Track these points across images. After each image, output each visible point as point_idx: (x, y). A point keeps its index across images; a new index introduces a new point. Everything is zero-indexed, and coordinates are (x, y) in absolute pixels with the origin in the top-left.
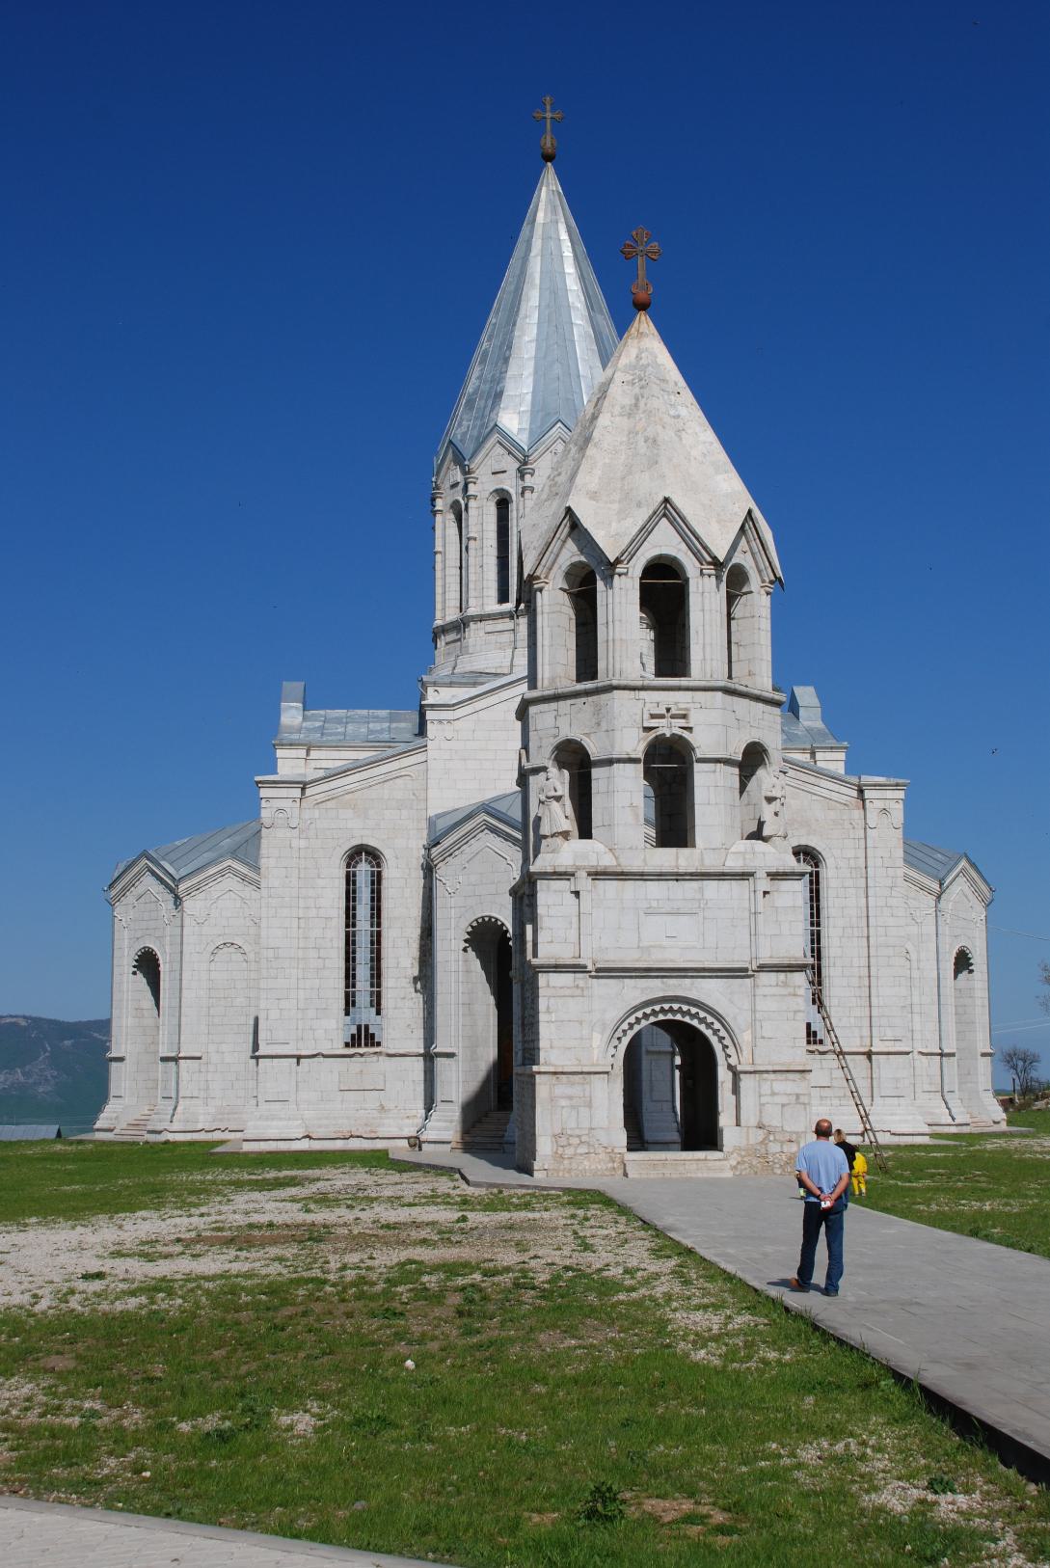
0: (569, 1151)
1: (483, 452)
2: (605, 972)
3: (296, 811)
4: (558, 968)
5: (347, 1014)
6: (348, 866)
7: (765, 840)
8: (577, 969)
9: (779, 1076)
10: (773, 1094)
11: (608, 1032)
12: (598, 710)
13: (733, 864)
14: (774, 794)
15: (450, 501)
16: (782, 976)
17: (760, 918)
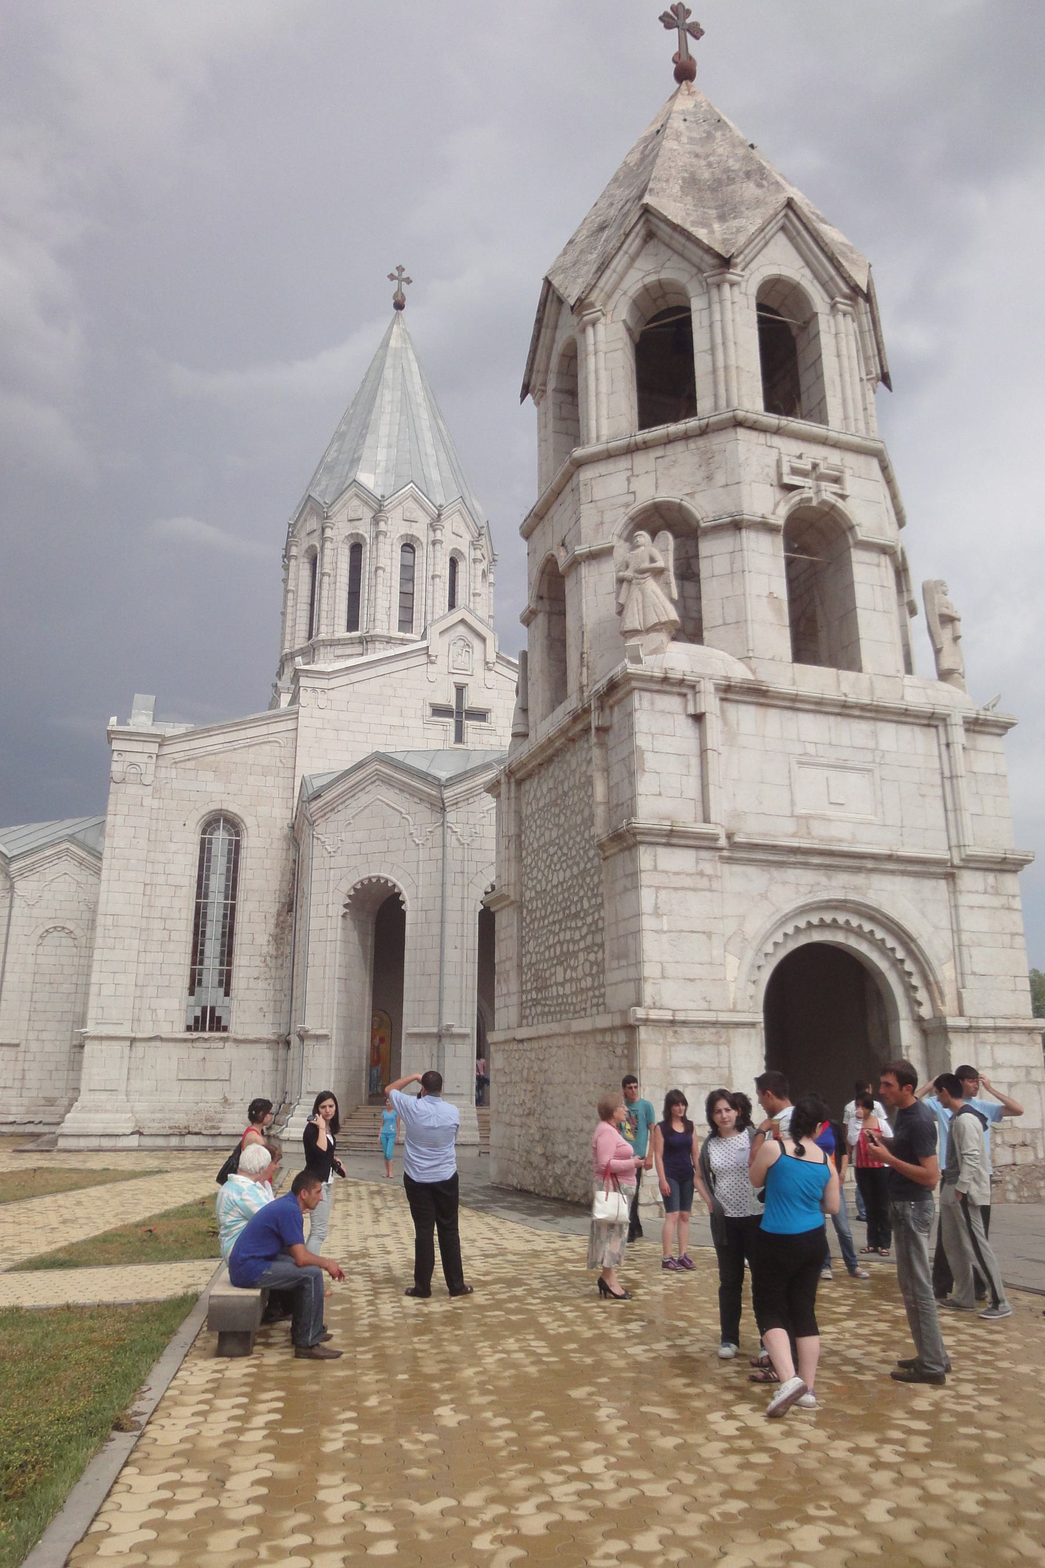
1: (341, 502)
2: (741, 851)
3: (151, 768)
4: (672, 837)
5: (192, 993)
6: (204, 832)
8: (703, 843)
9: (1004, 1038)
10: (996, 1066)
11: (750, 954)
12: (707, 459)
15: (305, 546)
16: (991, 878)
17: (962, 784)
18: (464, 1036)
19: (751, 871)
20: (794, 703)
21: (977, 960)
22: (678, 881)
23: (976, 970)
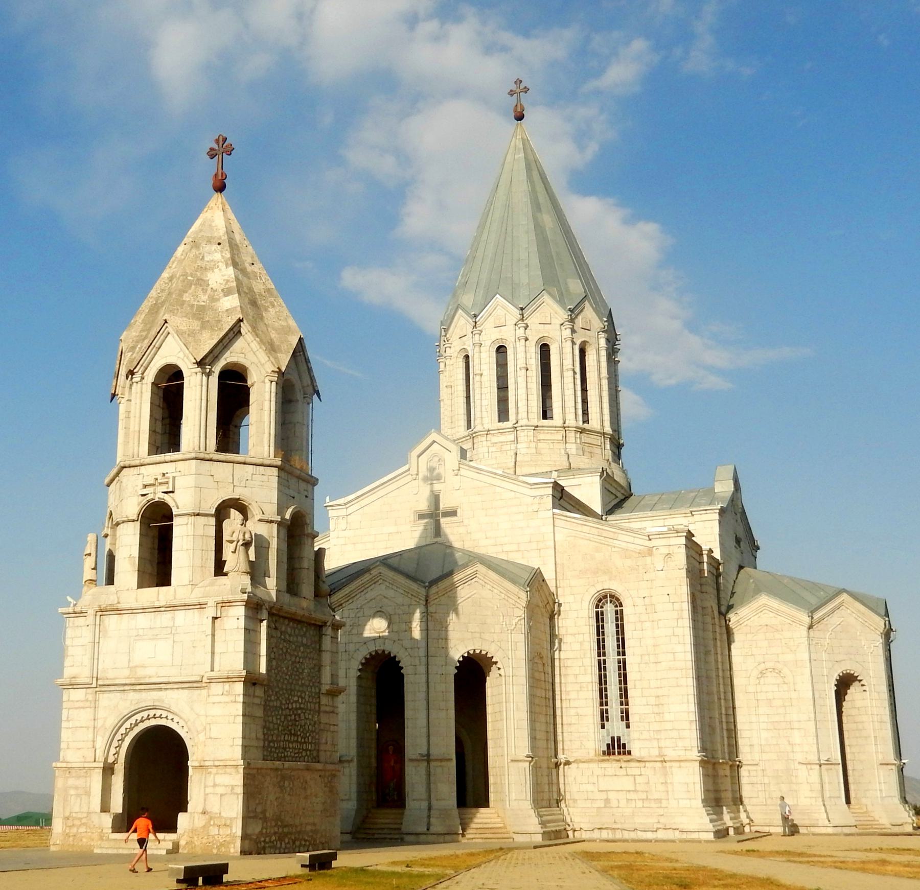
0: (74, 830)
7: (226, 574)
8: (86, 686)
10: (215, 785)
11: (108, 735)
13: (195, 597)
14: (235, 538)
16: (227, 685)
18: (349, 762)
19: (111, 695)
20: (132, 611)
22: (77, 705)
23: (212, 736)
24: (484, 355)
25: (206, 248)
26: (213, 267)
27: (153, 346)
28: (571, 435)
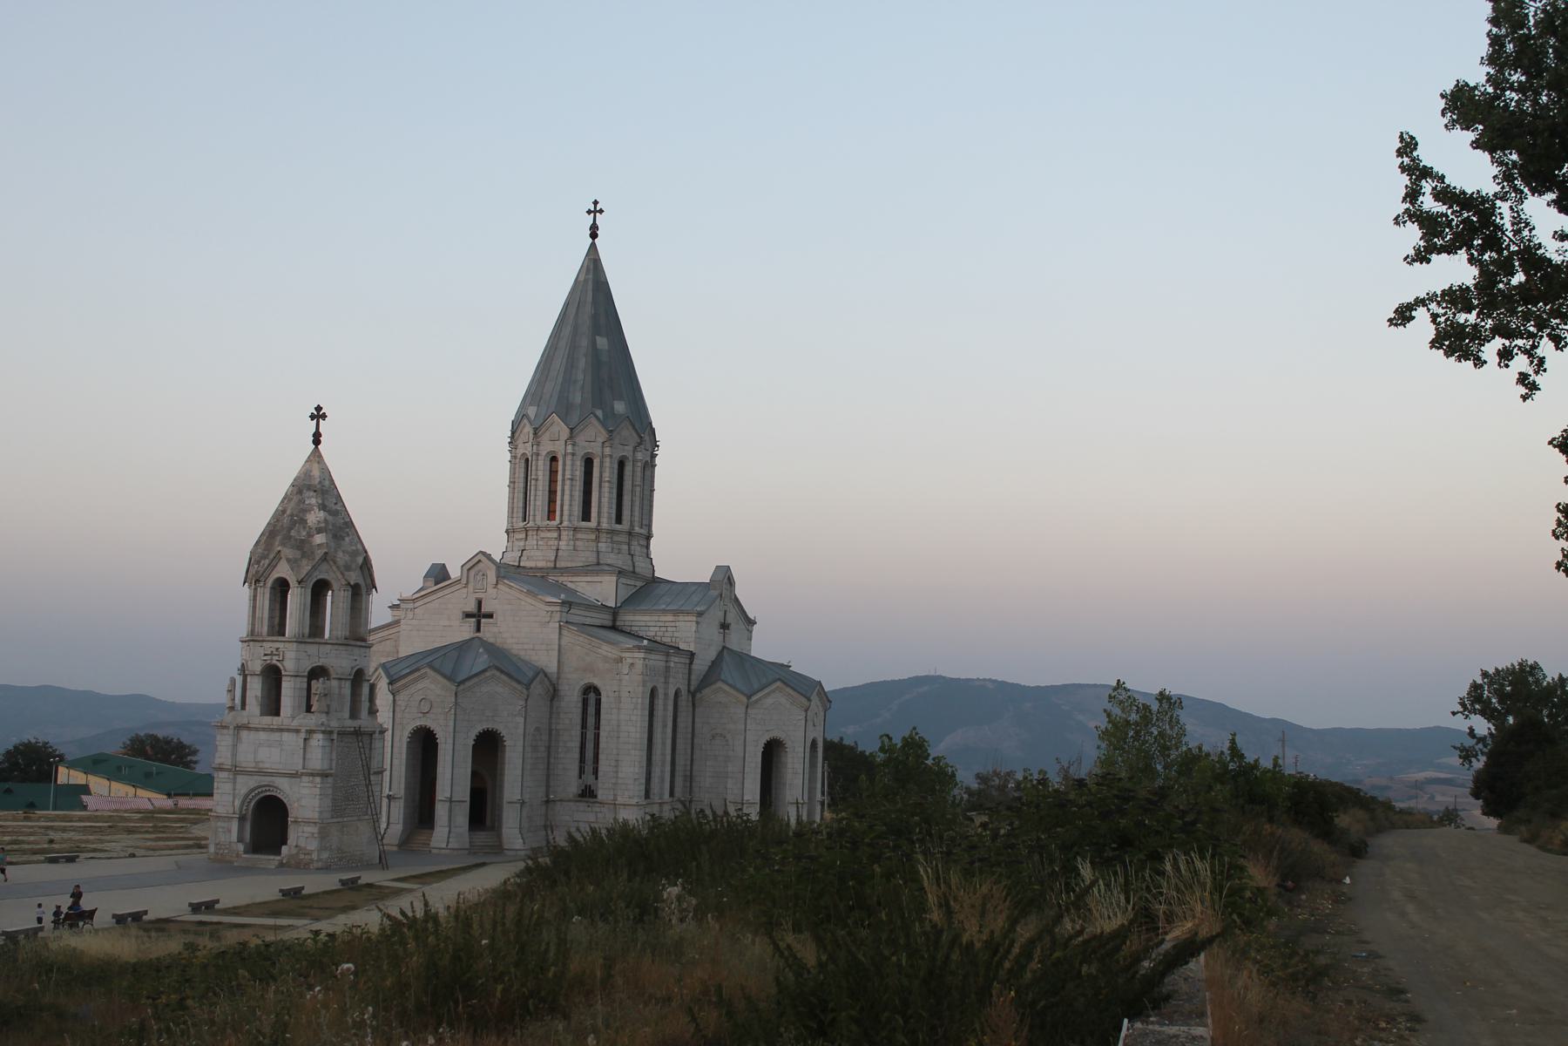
13: (295, 724)
20: (257, 729)
21: (303, 802)
24: (541, 463)
25: (307, 494)
26: (308, 510)
27: (272, 566)
28: (603, 537)
